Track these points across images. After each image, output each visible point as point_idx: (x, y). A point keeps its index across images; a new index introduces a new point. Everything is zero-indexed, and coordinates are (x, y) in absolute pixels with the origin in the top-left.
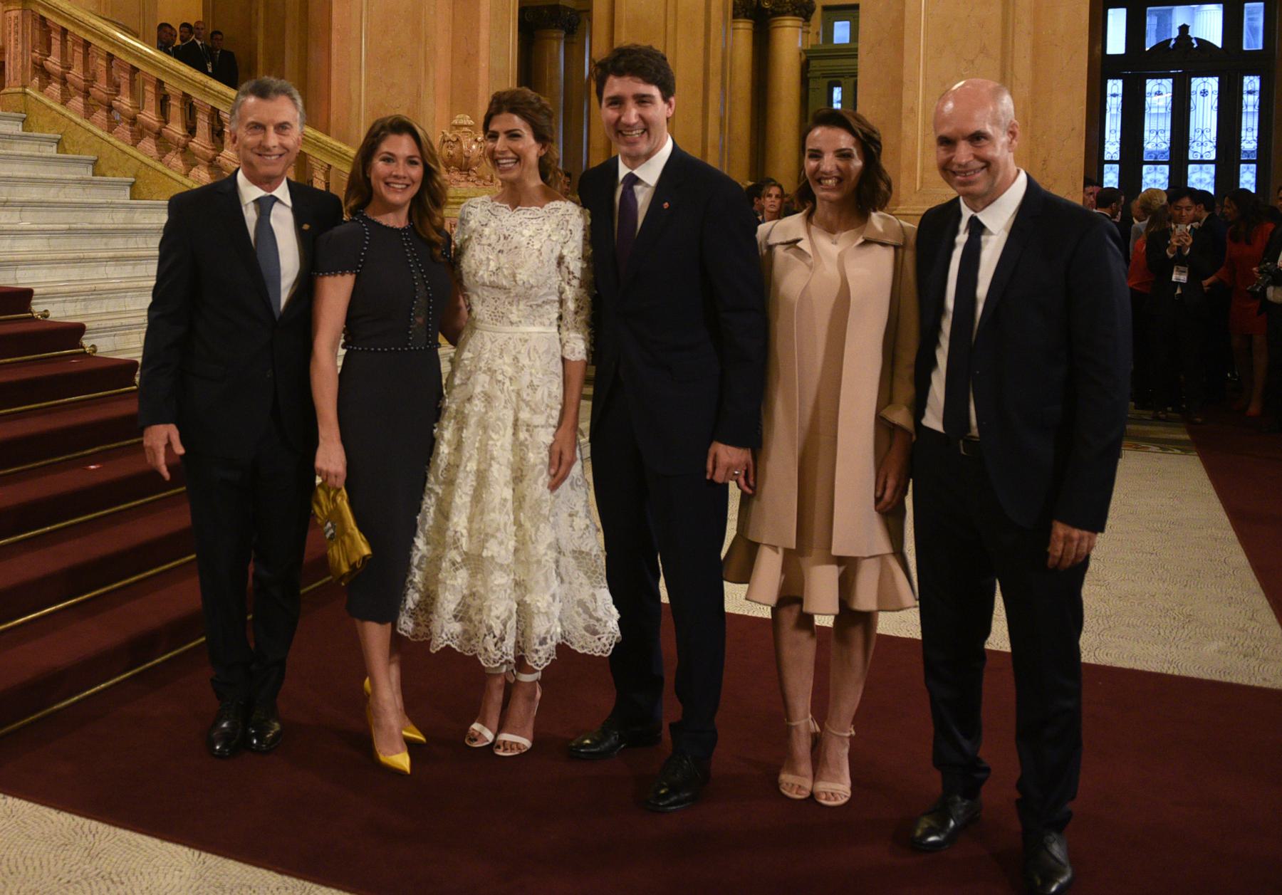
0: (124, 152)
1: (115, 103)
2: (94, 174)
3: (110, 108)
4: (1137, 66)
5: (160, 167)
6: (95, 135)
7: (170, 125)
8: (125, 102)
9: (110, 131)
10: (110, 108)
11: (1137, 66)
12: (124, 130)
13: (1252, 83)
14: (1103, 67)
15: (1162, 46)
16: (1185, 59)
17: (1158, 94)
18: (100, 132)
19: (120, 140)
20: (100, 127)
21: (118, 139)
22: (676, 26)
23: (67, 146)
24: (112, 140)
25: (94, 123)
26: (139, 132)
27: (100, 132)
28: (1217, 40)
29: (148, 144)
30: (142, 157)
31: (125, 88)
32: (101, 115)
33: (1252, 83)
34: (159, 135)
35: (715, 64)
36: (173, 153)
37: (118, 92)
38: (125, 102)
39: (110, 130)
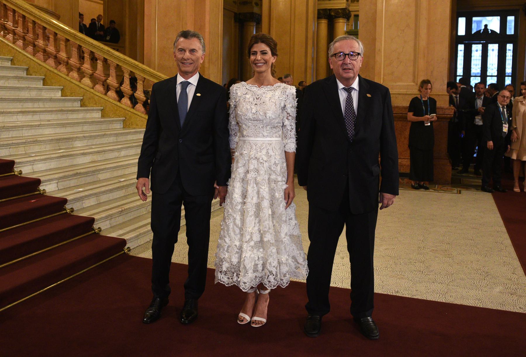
0: (40, 65)
1: (36, 43)
2: (27, 75)
3: (34, 46)
4: (470, 39)
5: (56, 71)
6: (28, 57)
7: (61, 53)
8: (41, 42)
9: (34, 56)
10: (34, 46)
11: (470, 39)
12: (40, 55)
13: (510, 47)
14: (455, 40)
15: (478, 32)
16: (486, 37)
17: (477, 49)
18: (29, 56)
19: (38, 59)
20: (30, 54)
21: (38, 59)
22: (295, 18)
23: (15, 62)
24: (34, 59)
25: (27, 52)
26: (47, 55)
27: (29, 56)
28: (498, 31)
29: (51, 61)
30: (48, 67)
31: (41, 36)
32: (30, 48)
33: (510, 47)
34: (56, 57)
35: (310, 35)
36: (62, 65)
37: (38, 38)
38: (41, 42)
39: (34, 55)
